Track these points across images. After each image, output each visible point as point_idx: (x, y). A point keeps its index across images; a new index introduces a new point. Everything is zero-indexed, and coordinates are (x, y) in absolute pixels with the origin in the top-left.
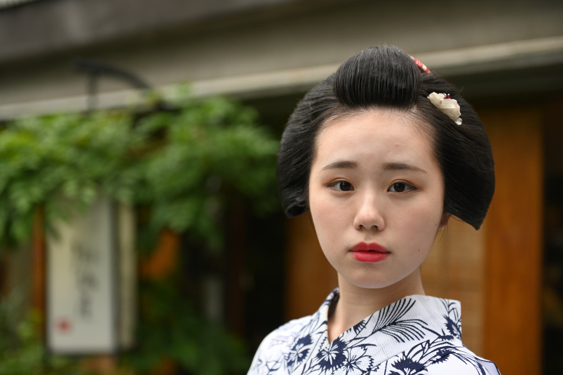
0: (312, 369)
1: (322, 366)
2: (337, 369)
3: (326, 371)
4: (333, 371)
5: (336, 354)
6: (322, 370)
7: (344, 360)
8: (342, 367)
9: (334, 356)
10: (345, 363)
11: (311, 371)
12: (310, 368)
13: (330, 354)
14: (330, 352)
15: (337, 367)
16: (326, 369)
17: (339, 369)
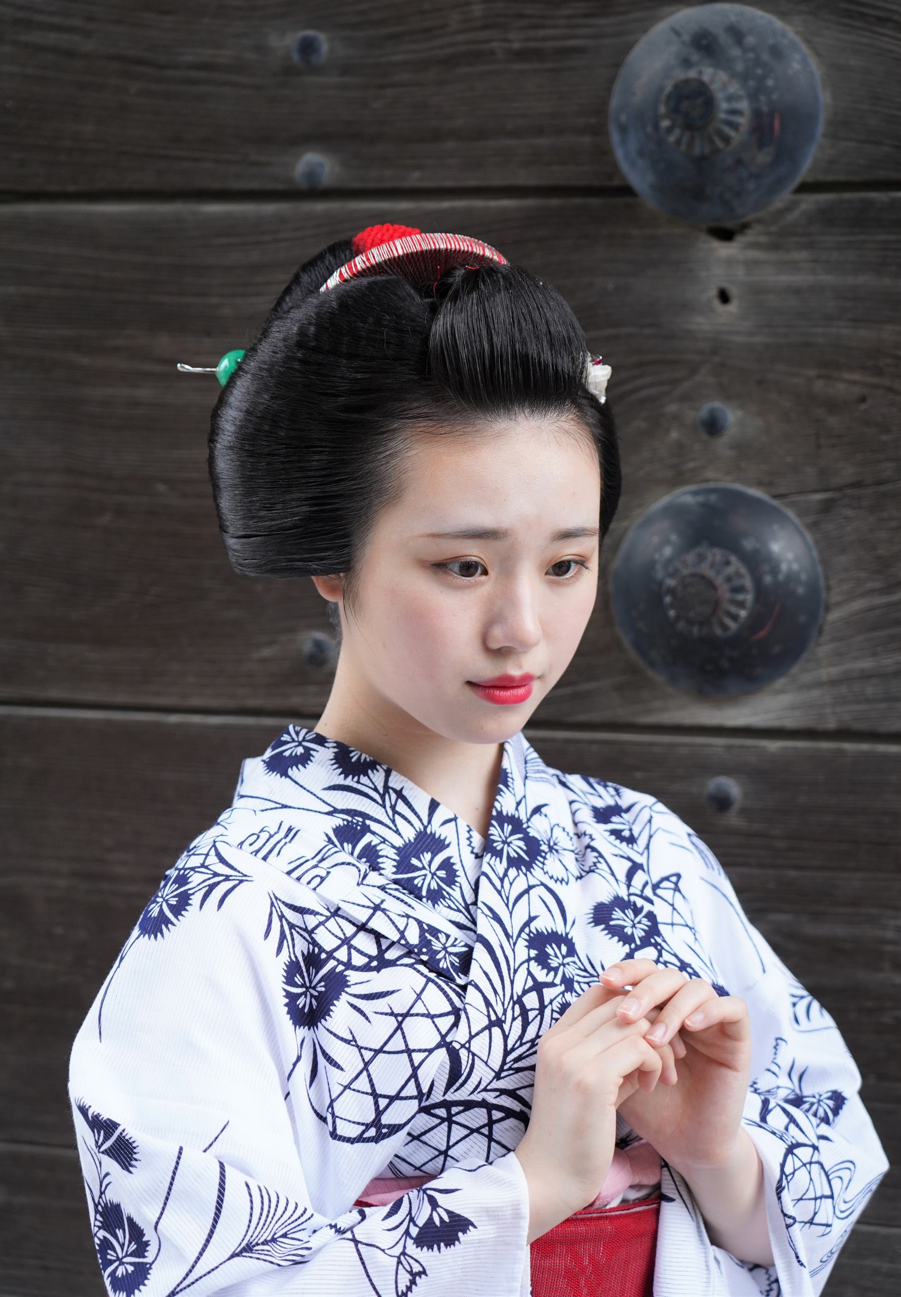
0: (506, 878)
1: (518, 868)
2: (543, 863)
3: (531, 873)
4: (543, 869)
5: (519, 839)
6: (526, 875)
7: (541, 845)
8: (548, 856)
9: (521, 844)
10: (544, 848)
11: (511, 884)
12: (502, 880)
13: (511, 842)
14: (509, 840)
15: (541, 859)
16: (528, 869)
17: (546, 862)
